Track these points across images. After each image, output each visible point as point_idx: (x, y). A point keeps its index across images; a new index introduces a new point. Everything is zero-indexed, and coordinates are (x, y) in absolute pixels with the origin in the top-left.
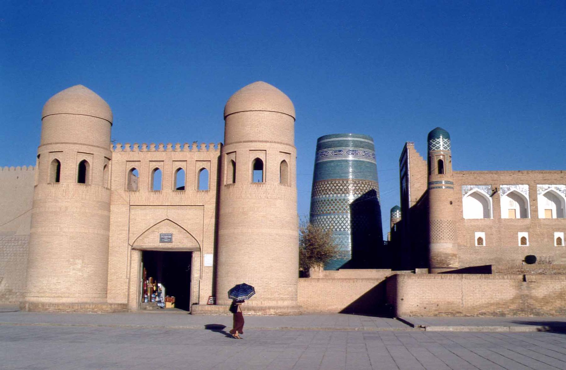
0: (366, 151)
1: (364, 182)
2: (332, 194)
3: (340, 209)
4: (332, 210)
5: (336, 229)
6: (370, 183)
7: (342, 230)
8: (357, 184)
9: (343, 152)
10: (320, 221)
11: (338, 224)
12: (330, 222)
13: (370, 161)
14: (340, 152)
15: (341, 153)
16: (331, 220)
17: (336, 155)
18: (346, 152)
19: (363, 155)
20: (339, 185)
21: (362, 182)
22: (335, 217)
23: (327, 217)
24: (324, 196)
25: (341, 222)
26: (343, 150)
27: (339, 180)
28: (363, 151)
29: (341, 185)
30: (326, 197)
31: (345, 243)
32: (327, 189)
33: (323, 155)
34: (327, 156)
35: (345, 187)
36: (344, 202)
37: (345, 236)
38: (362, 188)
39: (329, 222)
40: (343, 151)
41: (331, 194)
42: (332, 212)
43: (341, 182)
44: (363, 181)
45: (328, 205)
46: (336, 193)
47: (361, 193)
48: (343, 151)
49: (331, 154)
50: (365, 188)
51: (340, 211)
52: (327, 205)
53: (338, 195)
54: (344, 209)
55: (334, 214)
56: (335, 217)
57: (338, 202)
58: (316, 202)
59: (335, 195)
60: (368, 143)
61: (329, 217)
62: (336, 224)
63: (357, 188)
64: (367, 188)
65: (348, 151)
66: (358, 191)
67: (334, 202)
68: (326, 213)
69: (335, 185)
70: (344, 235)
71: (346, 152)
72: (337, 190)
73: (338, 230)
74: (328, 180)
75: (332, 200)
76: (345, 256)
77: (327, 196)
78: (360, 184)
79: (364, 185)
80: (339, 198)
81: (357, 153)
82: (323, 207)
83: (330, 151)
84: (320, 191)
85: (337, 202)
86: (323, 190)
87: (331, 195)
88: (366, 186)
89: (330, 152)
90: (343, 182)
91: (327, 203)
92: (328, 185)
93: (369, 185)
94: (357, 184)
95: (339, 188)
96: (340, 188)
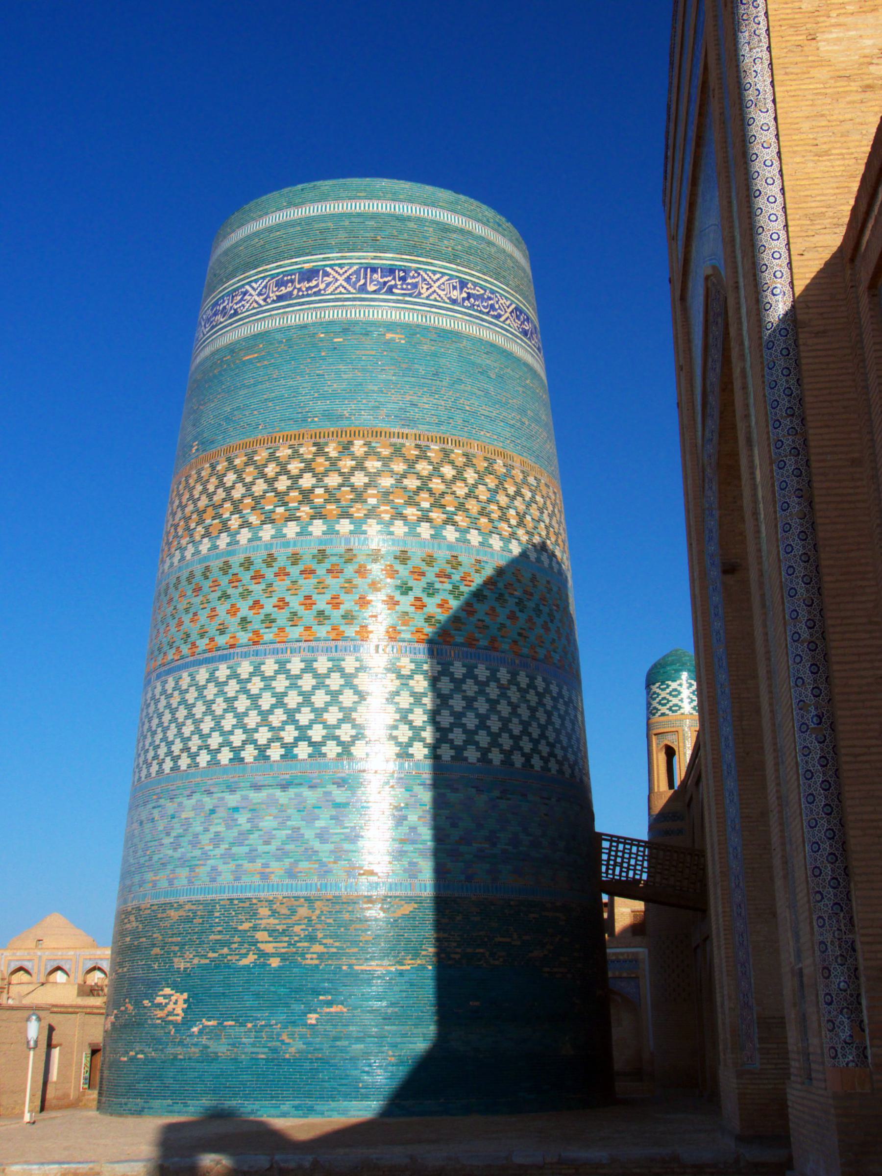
0: (475, 285)
3: (294, 618)
6: (500, 462)
7: (303, 751)
8: (412, 464)
9: (328, 279)
11: (278, 717)
13: (500, 341)
14: (309, 281)
15: (314, 283)
18: (348, 280)
21: (446, 453)
22: (257, 671)
23: (212, 674)
25: (300, 699)
26: (331, 266)
28: (451, 277)
29: (309, 468)
31: (316, 845)
32: (224, 500)
33: (219, 318)
34: (236, 313)
35: (333, 480)
36: (321, 570)
37: (320, 790)
38: (442, 487)
39: (219, 707)
40: (327, 274)
41: (246, 524)
42: (244, 637)
43: (307, 450)
44: (449, 446)
45: (225, 596)
46: (272, 521)
47: (433, 515)
48: (327, 274)
50: (461, 490)
52: (214, 596)
53: (285, 530)
54: (321, 613)
55: (257, 653)
56: (257, 671)
57: (282, 573)
59: (267, 533)
60: (490, 243)
62: (265, 715)
63: (412, 483)
64: (475, 486)
65: (357, 272)
66: (417, 504)
67: (258, 577)
68: (210, 650)
70: (312, 787)
71: (348, 280)
72: (282, 498)
73: (275, 753)
74: (230, 449)
75: (247, 564)
76: (312, 939)
78: (426, 458)
80: (290, 551)
81: (415, 286)
84: (187, 519)
85: (276, 575)
87: (245, 535)
88: (471, 476)
90: (320, 450)
92: (230, 478)
93: (489, 471)
94: (412, 464)
95: (290, 488)
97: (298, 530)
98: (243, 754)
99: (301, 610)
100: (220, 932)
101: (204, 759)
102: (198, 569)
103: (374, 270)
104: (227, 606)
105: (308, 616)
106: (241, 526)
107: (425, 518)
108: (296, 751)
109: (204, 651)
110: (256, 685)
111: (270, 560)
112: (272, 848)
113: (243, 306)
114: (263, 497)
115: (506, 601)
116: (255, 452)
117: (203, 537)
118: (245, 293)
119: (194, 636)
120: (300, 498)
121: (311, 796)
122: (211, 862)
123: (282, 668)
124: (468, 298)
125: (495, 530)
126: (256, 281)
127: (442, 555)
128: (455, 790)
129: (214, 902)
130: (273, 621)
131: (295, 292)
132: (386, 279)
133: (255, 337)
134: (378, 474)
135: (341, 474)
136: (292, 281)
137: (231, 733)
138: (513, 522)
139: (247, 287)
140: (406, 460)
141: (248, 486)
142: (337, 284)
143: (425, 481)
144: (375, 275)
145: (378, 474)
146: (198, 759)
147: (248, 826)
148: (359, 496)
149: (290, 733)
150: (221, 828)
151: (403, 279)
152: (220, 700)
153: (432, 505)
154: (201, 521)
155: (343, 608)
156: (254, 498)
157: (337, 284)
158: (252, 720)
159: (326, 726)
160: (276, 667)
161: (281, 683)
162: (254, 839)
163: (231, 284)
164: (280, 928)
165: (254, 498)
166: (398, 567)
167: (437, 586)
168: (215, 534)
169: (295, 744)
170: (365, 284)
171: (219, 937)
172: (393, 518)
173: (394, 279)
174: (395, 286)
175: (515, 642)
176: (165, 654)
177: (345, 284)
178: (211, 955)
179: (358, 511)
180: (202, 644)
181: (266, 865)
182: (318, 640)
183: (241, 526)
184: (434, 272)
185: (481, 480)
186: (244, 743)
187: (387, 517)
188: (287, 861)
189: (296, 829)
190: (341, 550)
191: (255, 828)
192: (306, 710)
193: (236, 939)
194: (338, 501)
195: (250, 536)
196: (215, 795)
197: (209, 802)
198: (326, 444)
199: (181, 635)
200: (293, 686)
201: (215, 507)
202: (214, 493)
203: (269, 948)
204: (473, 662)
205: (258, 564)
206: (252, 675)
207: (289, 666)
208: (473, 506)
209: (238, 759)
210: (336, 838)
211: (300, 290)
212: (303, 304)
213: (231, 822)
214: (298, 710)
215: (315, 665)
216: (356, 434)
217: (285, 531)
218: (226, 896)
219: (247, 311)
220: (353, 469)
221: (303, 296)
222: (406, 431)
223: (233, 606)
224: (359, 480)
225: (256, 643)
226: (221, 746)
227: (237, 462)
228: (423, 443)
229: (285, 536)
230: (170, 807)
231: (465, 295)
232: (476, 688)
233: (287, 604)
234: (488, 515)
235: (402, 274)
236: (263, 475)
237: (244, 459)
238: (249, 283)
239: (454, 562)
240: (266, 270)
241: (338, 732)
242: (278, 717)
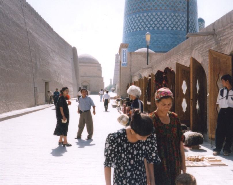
4: (153, 6)
10: (139, 19)
11: (161, 22)
12: (152, 20)
16: (152, 17)
22: (156, 14)
42: (154, 8)
56: (156, 14)
61: (150, 14)
73: (160, 28)
108: (164, 28)
110: (156, 17)
119: (143, 7)
123: (161, 14)
137: (152, 24)
147: (156, 40)
152: (149, 19)
159: (169, 24)
160: (160, 14)
169: (164, 27)
182: (167, 10)
189: (164, 41)
206: (155, 15)
223: (151, 3)
225: (156, 9)
242: (161, 22)
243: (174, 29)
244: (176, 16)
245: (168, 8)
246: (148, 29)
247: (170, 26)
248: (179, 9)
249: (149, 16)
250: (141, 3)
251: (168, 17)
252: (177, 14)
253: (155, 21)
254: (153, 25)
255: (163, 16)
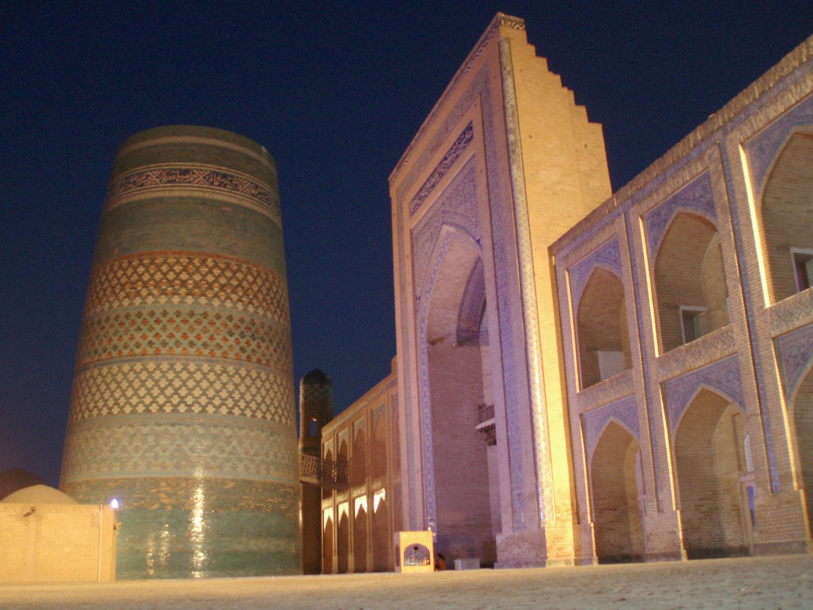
0: (262, 188)
1: (254, 269)
2: (153, 295)
3: (178, 344)
5: (161, 408)
6: (271, 276)
7: (182, 408)
8: (234, 273)
9: (195, 176)
10: (108, 380)
15: (187, 177)
17: (174, 181)
18: (205, 178)
19: (253, 195)
20: (177, 268)
21: (249, 269)
22: (158, 368)
24: (126, 302)
25: (181, 383)
26: (197, 170)
27: (178, 253)
28: (252, 183)
29: (185, 269)
30: (132, 304)
31: (189, 453)
32: (138, 281)
34: (142, 185)
35: (197, 277)
36: (192, 321)
37: (191, 428)
40: (194, 173)
41: (150, 294)
42: (150, 351)
44: (251, 266)
45: (139, 329)
46: (166, 294)
48: (194, 173)
49: (158, 181)
50: (255, 288)
51: (175, 349)
52: (132, 329)
53: (173, 300)
55: (158, 359)
56: (158, 368)
57: (171, 321)
58: (99, 322)
59: (163, 300)
61: (138, 367)
65: (209, 175)
66: (236, 293)
67: (158, 321)
68: (131, 356)
69: (164, 268)
70: (187, 426)
71: (205, 178)
72: (171, 283)
73: (168, 408)
74: (141, 255)
75: (152, 314)
77: (138, 301)
79: (253, 277)
80: (176, 310)
81: (236, 185)
82: (121, 336)
83: (154, 173)
84: (113, 288)
85: (168, 321)
86: (123, 287)
87: (150, 300)
88: (259, 281)
89: (153, 176)
90: (191, 262)
91: (133, 323)
92: (141, 270)
94: (234, 273)
95: (175, 279)
96: (180, 280)
97: (180, 300)
98: (151, 408)
99: (181, 340)
100: (140, 493)
101: (128, 409)
102: (122, 315)
103: (217, 174)
104: (141, 334)
105: (185, 343)
106: (148, 295)
107: (240, 300)
108: (179, 408)
109: (127, 356)
111: (165, 313)
112: (167, 454)
113: (147, 182)
114: (161, 281)
115: (272, 343)
116: (156, 258)
117: (125, 298)
118: (148, 176)
119: (121, 347)
120: (181, 284)
121: (187, 431)
122: (134, 460)
123: (172, 367)
124: (258, 194)
125: (269, 309)
126: (155, 171)
127: (248, 319)
128: (252, 431)
129: (136, 479)
130: (166, 344)
131: (177, 180)
132: (223, 180)
133: (155, 199)
134: (219, 276)
135: (201, 275)
136: (176, 174)
137: (144, 397)
138: (276, 305)
139: (150, 173)
140: (232, 271)
141: (152, 275)
142: (199, 179)
143: (240, 282)
144: (218, 178)
145: (219, 276)
146: (113, 410)
147: (154, 443)
148: (210, 287)
149: (175, 400)
150: (139, 444)
151: (231, 181)
153: (244, 294)
154: (122, 289)
155: (202, 340)
156: (156, 282)
157: (199, 179)
158: (156, 391)
159: (194, 397)
161: (185, 375)
162: (158, 449)
163: (141, 169)
164: (172, 492)
165: (156, 282)
166: (228, 322)
167: (245, 333)
168: (132, 297)
169: (178, 404)
170: (213, 181)
171: (139, 496)
172: (226, 299)
173: (227, 180)
174: (227, 184)
175: (276, 363)
176: (100, 355)
177: (203, 179)
178: (134, 504)
179: (210, 294)
180: (126, 352)
181: (164, 462)
182: (189, 355)
183: (148, 295)
184: (245, 180)
185: (263, 284)
186: (152, 403)
187: (223, 298)
188: (175, 461)
189: (179, 446)
190: (202, 312)
191: (157, 444)
192: (184, 388)
193: (148, 497)
194: (199, 288)
195: (153, 300)
196: (135, 427)
197: (131, 431)
198: (194, 259)
199: (111, 346)
200: (177, 376)
201: (132, 283)
202: (131, 276)
203: (166, 501)
204: (260, 370)
205: (158, 314)
206: (155, 370)
207: (175, 367)
208: (260, 296)
209: (147, 411)
210: (199, 451)
211: (180, 179)
212: (182, 186)
213: (144, 441)
214: (180, 388)
215: (189, 367)
216: (209, 255)
217: (173, 300)
218: (143, 476)
219: (150, 185)
220: (207, 273)
221: (181, 183)
222: (232, 256)
224: (210, 278)
225: (157, 354)
226: (138, 403)
227: (145, 262)
228: (240, 264)
229: (172, 302)
230: (108, 433)
231: (257, 192)
232: (261, 383)
233: (174, 336)
234: (266, 301)
235: (230, 179)
236: (160, 270)
237: (149, 261)
238: (151, 171)
239: (242, 321)
240: (160, 166)
241: (200, 400)
243: (210, 409)
244: (216, 374)
245: (192, 351)
246: (131, 409)
247: (196, 402)
248: (225, 353)
249: (135, 373)
250: (115, 334)
251: (191, 375)
252: (218, 368)
253: (152, 388)
254: (148, 400)
255: (178, 374)
